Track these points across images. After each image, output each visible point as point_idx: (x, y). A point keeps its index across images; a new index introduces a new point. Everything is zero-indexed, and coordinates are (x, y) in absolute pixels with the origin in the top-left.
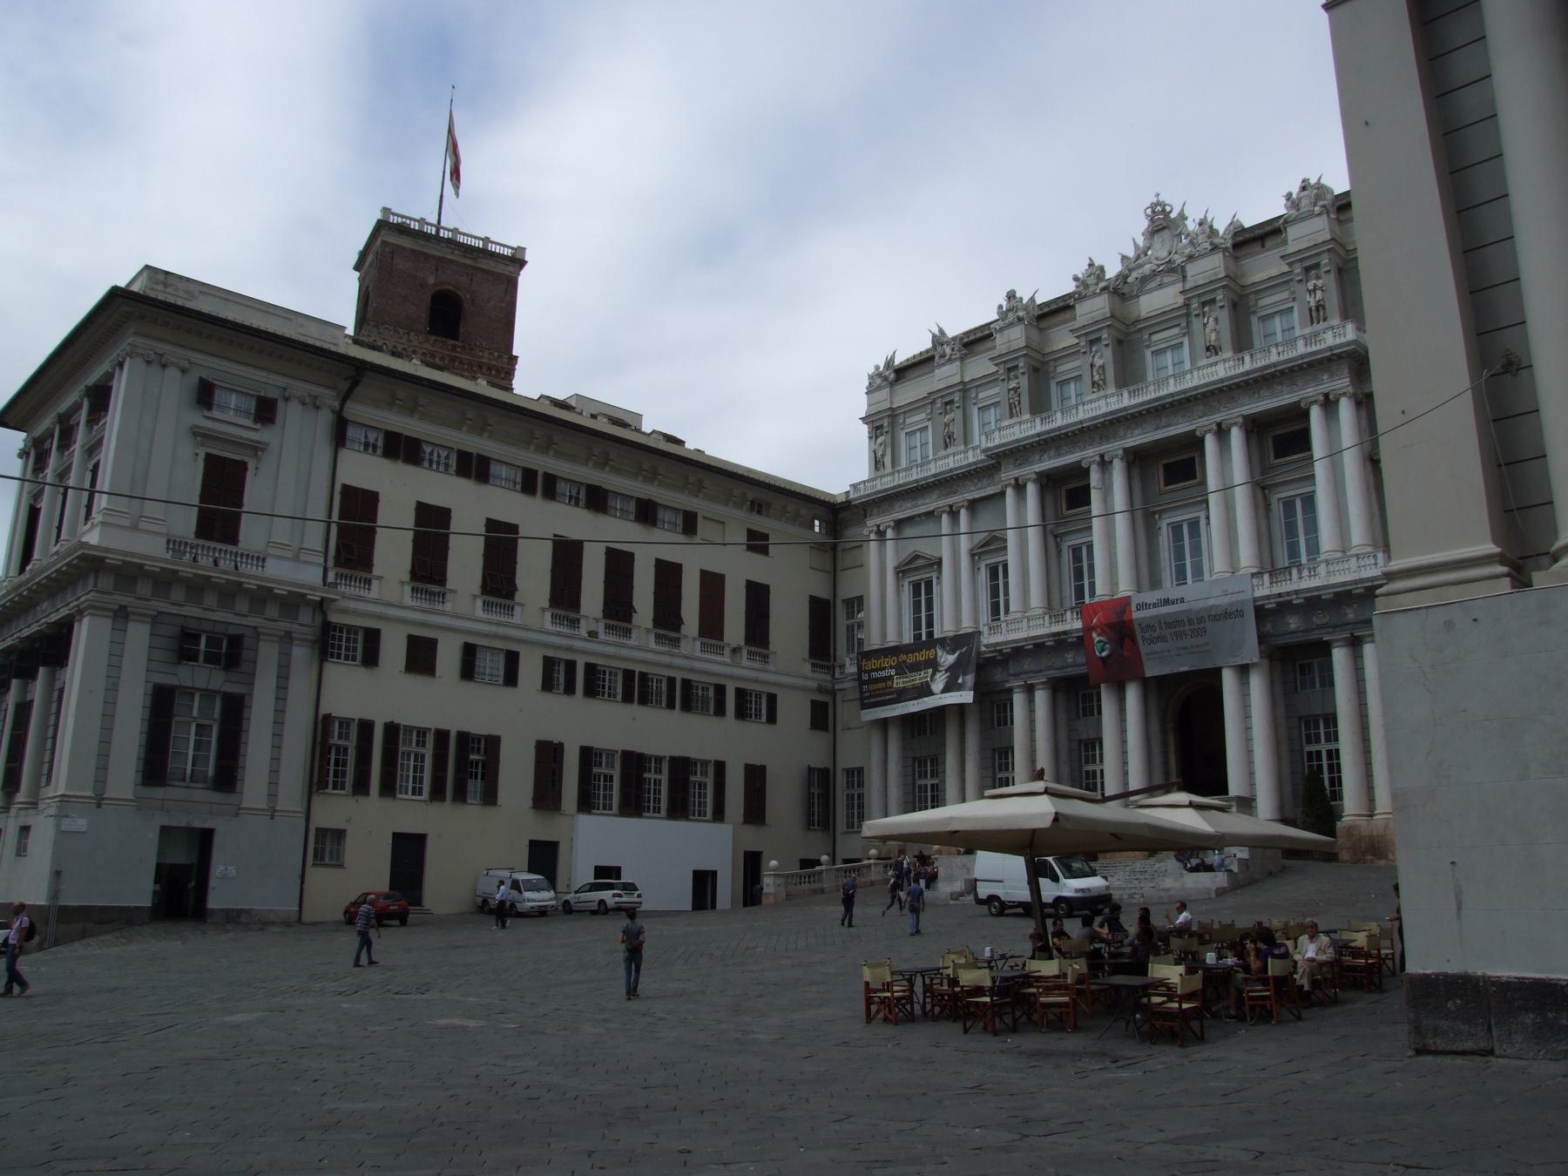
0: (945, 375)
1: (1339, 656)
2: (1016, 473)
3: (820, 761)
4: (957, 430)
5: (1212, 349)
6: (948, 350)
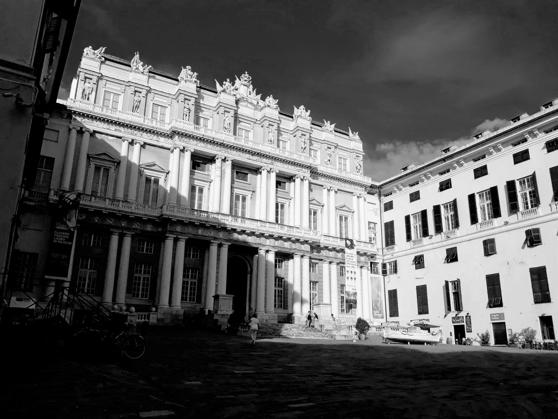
2: (185, 145)
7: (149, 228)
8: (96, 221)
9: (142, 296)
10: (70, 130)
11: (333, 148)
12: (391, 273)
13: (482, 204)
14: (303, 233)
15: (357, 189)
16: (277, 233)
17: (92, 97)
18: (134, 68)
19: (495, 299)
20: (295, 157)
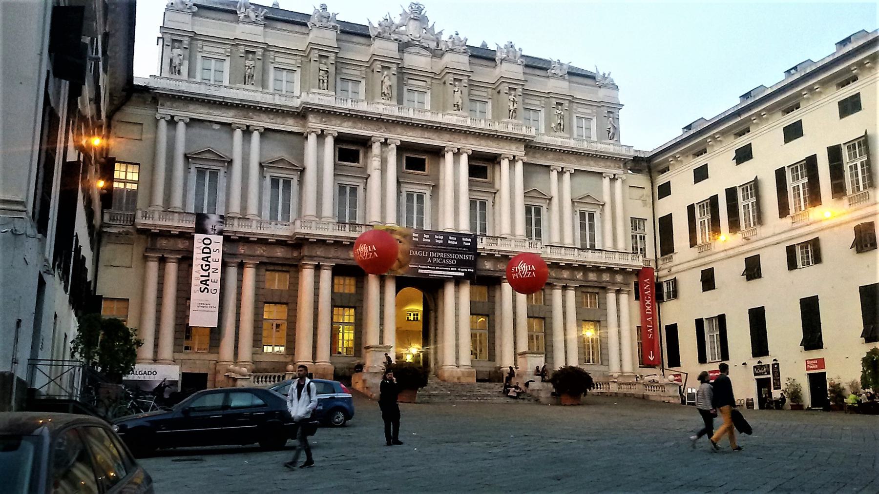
2: (323, 127)
5: (457, 107)
6: (252, 15)
10: (157, 121)
11: (566, 103)
12: (669, 297)
13: (796, 184)
14: (513, 245)
17: (184, 69)
18: (242, 16)
19: (812, 338)
20: (498, 127)
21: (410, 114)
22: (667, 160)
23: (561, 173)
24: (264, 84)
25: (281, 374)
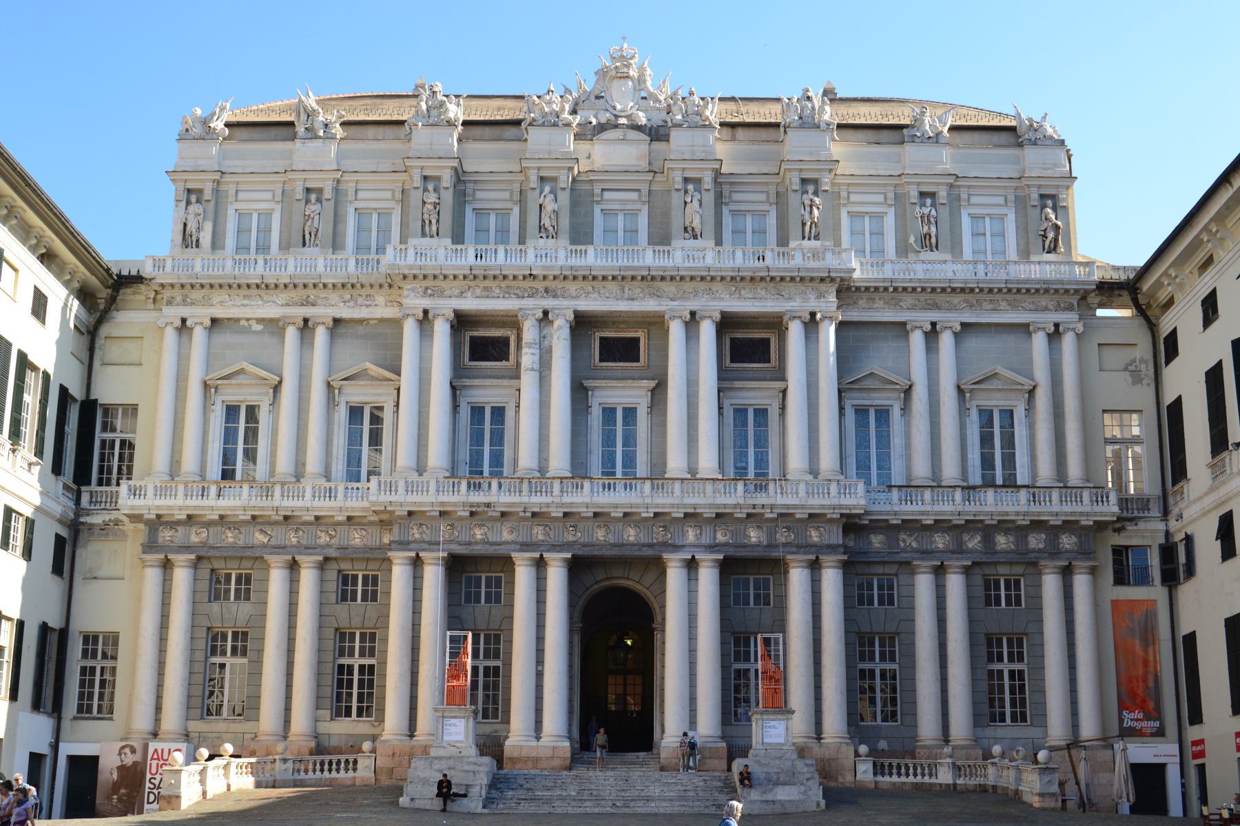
0: (315, 158)
1: (797, 578)
3: (55, 622)
4: (326, 229)
7: (357, 538)
8: (231, 540)
9: (359, 714)
10: (162, 329)
14: (802, 493)
15: (1046, 309)
16: (711, 506)
17: (206, 237)
20: (773, 261)
21: (592, 258)
22: (1159, 284)
23: (932, 334)
24: (336, 244)
25: (351, 758)
